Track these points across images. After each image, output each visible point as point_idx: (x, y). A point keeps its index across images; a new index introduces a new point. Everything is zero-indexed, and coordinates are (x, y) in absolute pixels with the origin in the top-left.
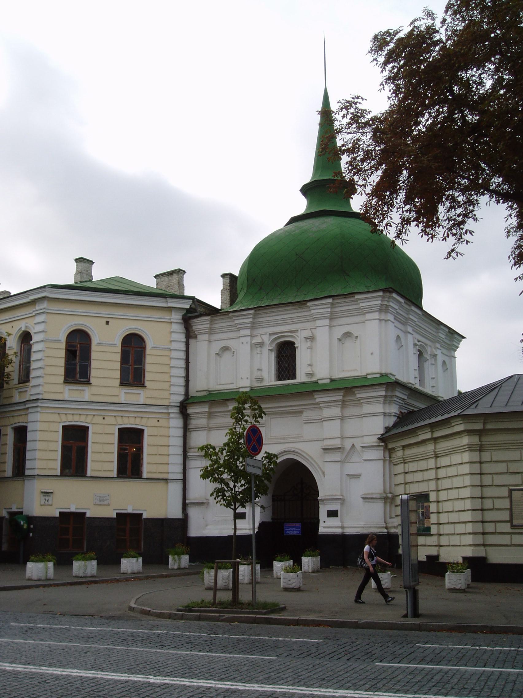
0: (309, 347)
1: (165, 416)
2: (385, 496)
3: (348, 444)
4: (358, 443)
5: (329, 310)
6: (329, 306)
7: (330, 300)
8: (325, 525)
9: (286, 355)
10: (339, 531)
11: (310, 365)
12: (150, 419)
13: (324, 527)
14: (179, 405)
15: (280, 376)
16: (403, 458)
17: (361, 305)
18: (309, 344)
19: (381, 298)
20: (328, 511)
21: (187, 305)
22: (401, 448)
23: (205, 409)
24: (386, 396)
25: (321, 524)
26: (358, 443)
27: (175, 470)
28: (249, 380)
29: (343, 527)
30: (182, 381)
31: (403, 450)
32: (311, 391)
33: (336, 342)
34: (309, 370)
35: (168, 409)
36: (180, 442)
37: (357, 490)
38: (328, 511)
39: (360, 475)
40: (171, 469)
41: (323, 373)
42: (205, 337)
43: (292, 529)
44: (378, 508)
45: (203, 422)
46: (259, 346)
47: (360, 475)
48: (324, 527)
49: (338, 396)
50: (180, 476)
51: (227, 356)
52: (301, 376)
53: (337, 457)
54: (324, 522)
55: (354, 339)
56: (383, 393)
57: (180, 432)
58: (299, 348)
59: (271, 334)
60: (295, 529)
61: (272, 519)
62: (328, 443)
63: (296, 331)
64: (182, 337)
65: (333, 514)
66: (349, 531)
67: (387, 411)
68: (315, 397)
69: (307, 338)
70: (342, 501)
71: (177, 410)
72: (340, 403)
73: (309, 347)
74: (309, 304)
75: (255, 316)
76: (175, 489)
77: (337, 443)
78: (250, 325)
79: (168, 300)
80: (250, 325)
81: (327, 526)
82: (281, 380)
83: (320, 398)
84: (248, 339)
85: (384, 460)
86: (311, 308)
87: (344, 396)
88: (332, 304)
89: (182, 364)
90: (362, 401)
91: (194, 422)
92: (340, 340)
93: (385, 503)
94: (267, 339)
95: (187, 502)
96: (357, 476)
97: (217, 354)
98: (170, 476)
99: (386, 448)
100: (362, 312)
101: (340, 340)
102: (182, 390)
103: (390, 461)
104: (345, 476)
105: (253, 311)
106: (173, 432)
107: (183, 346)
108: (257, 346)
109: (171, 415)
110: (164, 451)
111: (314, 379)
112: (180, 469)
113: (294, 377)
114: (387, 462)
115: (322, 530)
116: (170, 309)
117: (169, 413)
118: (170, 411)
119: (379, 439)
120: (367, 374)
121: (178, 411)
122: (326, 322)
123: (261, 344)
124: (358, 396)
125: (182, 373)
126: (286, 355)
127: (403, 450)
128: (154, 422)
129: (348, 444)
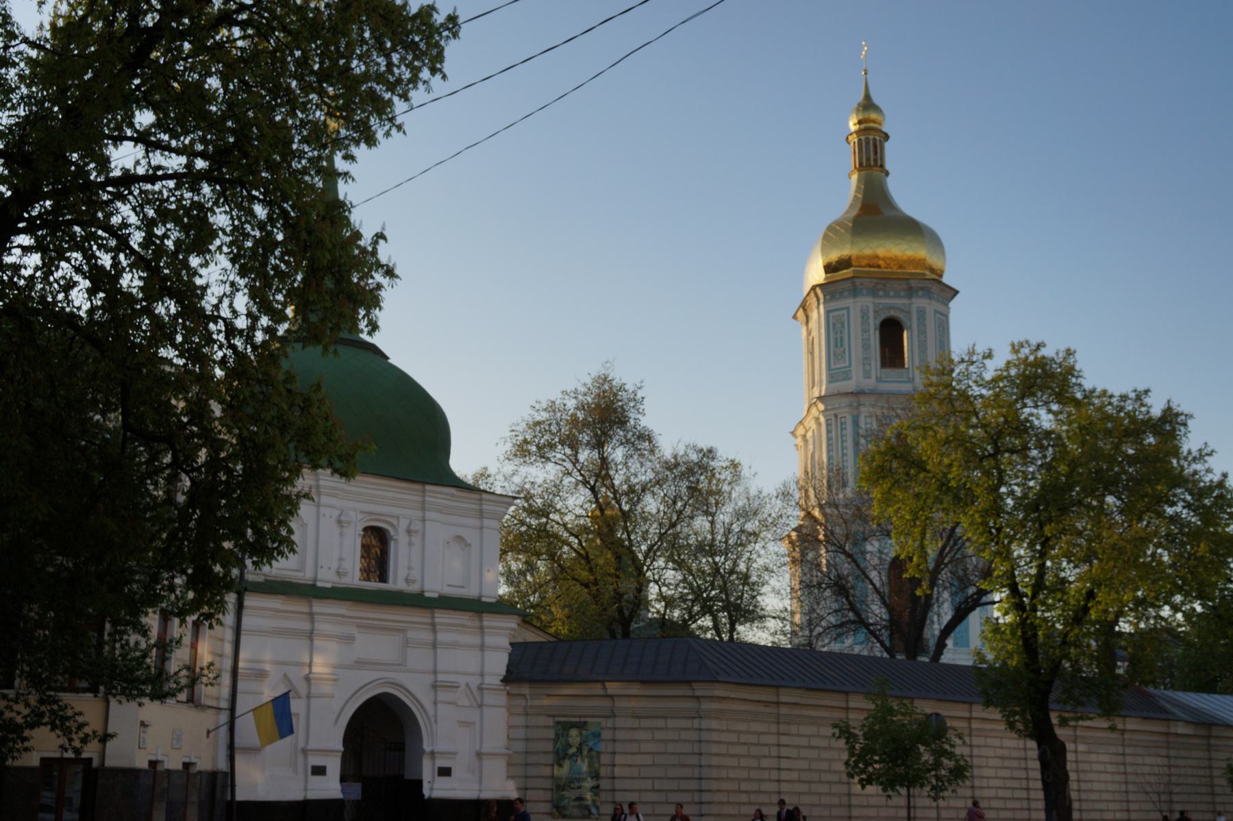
4: (475, 682)
9: (377, 545)
15: (367, 573)
32: (417, 601)
47: (473, 723)
52: (397, 581)
59: (362, 512)
62: (440, 677)
65: (445, 772)
74: (428, 487)
81: (435, 788)
82: (369, 580)
83: (442, 617)
99: (508, 694)
111: (414, 588)
113: (383, 578)
126: (377, 545)
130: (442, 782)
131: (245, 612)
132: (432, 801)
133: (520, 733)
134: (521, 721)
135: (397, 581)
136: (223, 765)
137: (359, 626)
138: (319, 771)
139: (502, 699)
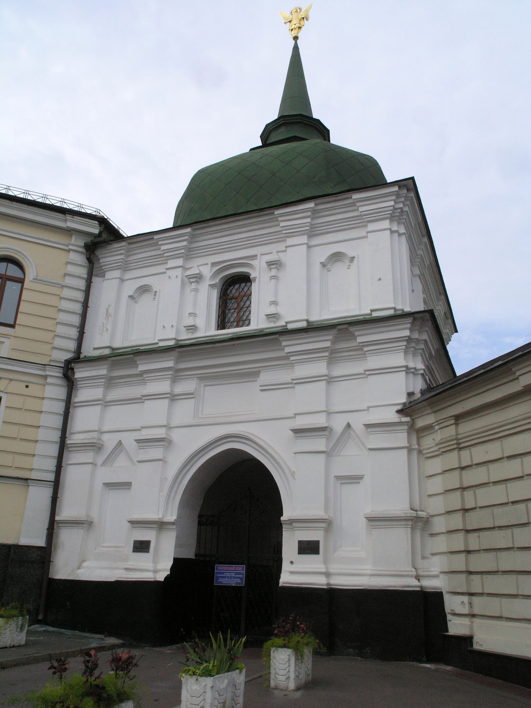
0: (273, 277)
1: (41, 381)
2: (414, 514)
3: (338, 424)
4: (358, 422)
5: (309, 220)
6: (309, 214)
7: (311, 205)
8: (293, 568)
10: (319, 581)
11: (274, 303)
12: (13, 383)
13: (291, 573)
14: (62, 365)
16: (457, 439)
17: (361, 209)
18: (274, 272)
19: (394, 197)
20: (300, 542)
21: (94, 229)
22: (453, 422)
23: (102, 370)
24: (409, 340)
25: (286, 566)
26: (358, 422)
27: (43, 465)
28: (174, 329)
29: (327, 574)
30: (74, 333)
31: (457, 424)
33: (317, 268)
34: (272, 310)
35: (45, 370)
36: (58, 422)
37: (356, 506)
38: (300, 542)
39: (361, 477)
40: (36, 463)
41: (294, 314)
42: (116, 274)
43: (228, 575)
44: (400, 538)
45: (97, 393)
46: (194, 280)
47: (361, 477)
48: (291, 573)
49: (324, 342)
50: (51, 477)
51: (146, 298)
53: (319, 443)
54: (292, 562)
55: (347, 262)
56: (407, 333)
57: (60, 407)
58: (257, 280)
59: (214, 264)
60: (233, 575)
61: (196, 555)
62: (302, 422)
63: (254, 257)
64: (83, 272)
65: (309, 548)
66: (343, 581)
67: (411, 365)
68: (284, 344)
69: (270, 264)
70: (328, 524)
71: (59, 373)
72: (327, 354)
73: (273, 277)
75: (192, 239)
76: (40, 496)
77: (320, 421)
78: (183, 251)
79: (69, 217)
80: (183, 251)
81: (296, 571)
82: (224, 328)
84: (179, 271)
85: (410, 450)
86: (280, 219)
87: (334, 343)
88: (314, 212)
89: (78, 308)
90: (365, 349)
91: (82, 394)
92: (323, 265)
93: (413, 529)
94: (207, 271)
95: (57, 518)
96: (356, 479)
97: (131, 297)
98: (34, 475)
99: (411, 428)
100: (362, 221)
101: (323, 265)
102: (72, 345)
103: (420, 452)
104: (332, 480)
105: (189, 230)
106: (46, 406)
107: (82, 284)
108: (192, 280)
109: (49, 380)
110: (29, 433)
111: (281, 323)
112: (51, 465)
114: (415, 453)
115: (287, 578)
116: (70, 232)
117: (45, 377)
118: (48, 373)
119: (398, 412)
120: (372, 311)
121: (61, 375)
122: (304, 239)
123: (198, 278)
124: (360, 340)
125: (76, 320)
127: (457, 424)
128: (19, 388)
129: (338, 424)
130: (310, 562)
131: (80, 384)
132: (284, 588)
133: (437, 485)
134: (435, 465)
135: (258, 322)
136: (40, 542)
137: (202, 378)
138: (141, 547)
139: (401, 438)
